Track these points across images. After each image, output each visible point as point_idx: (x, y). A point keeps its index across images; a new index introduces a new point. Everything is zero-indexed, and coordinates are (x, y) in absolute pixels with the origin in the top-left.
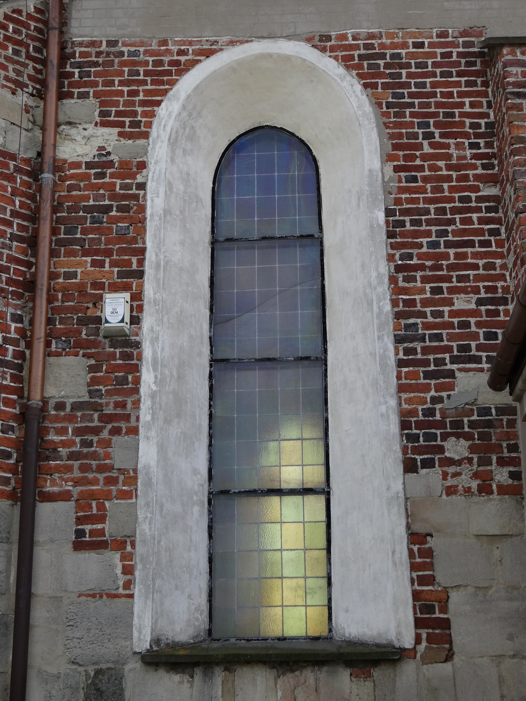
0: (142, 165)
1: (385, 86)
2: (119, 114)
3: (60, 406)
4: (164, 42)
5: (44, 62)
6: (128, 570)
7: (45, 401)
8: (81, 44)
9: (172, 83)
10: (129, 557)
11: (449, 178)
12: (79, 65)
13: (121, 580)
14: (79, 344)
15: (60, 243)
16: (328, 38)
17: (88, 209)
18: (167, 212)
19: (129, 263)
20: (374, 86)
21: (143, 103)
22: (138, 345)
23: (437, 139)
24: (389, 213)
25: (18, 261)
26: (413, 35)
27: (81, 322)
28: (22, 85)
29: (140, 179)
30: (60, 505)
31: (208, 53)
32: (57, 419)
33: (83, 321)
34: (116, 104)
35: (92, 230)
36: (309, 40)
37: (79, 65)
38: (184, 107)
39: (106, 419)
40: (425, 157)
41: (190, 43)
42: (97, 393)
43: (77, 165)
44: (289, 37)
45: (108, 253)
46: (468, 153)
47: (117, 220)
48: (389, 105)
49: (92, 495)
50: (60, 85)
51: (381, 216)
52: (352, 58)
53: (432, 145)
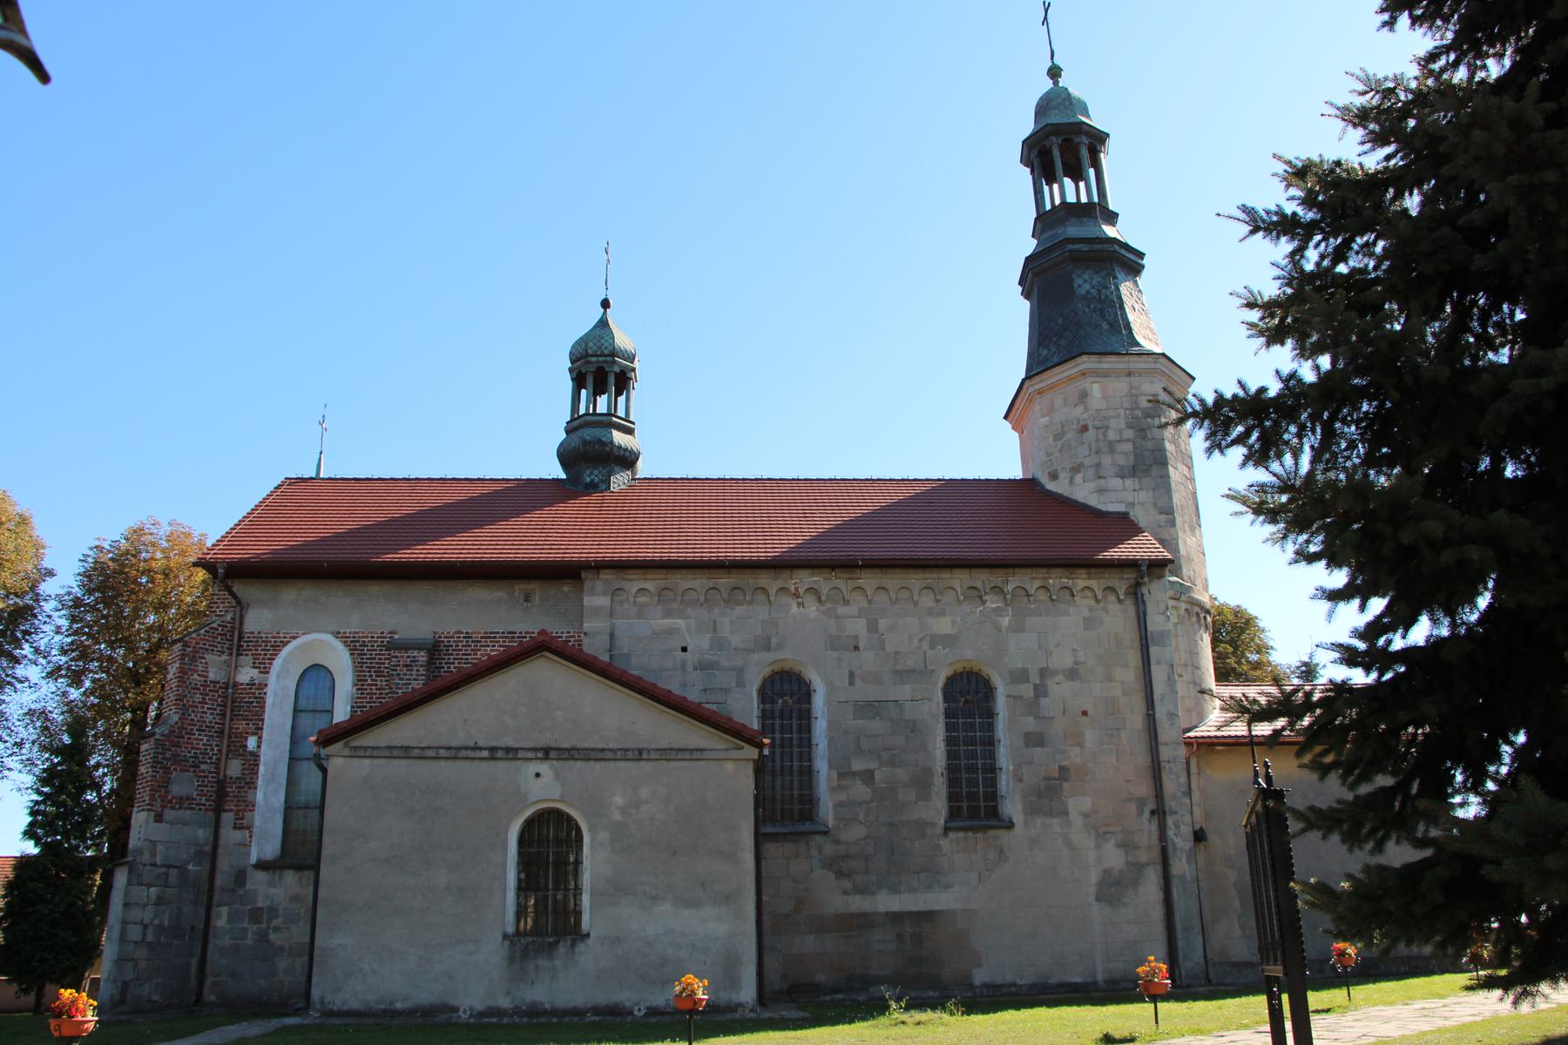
0: (266, 685)
1: (358, 654)
2: (260, 663)
3: (231, 778)
4: (278, 633)
5: (232, 641)
6: (251, 837)
7: (225, 776)
8: (248, 633)
9: (280, 650)
10: (251, 832)
11: (375, 694)
12: (246, 642)
13: (249, 839)
14: (240, 755)
15: (235, 715)
16: (340, 633)
17: (246, 702)
18: (274, 704)
19: (258, 724)
20: (354, 654)
21: (268, 659)
22: (259, 756)
23: (374, 678)
24: (352, 707)
25: (219, 724)
26: (370, 633)
27: (241, 746)
28: (223, 652)
29: (265, 691)
30: (230, 814)
31: (294, 638)
32: (230, 783)
33: (241, 746)
34: (259, 659)
35: (246, 711)
36: (332, 633)
37: (246, 642)
38: (283, 661)
39: (246, 783)
40: (369, 685)
41: (288, 633)
42: (243, 774)
43: (242, 684)
44: (326, 632)
45: (251, 720)
46: (384, 684)
47: (255, 707)
48: (359, 663)
49: (240, 810)
50: (238, 650)
51: (349, 708)
52: (347, 642)
53: (372, 680)
